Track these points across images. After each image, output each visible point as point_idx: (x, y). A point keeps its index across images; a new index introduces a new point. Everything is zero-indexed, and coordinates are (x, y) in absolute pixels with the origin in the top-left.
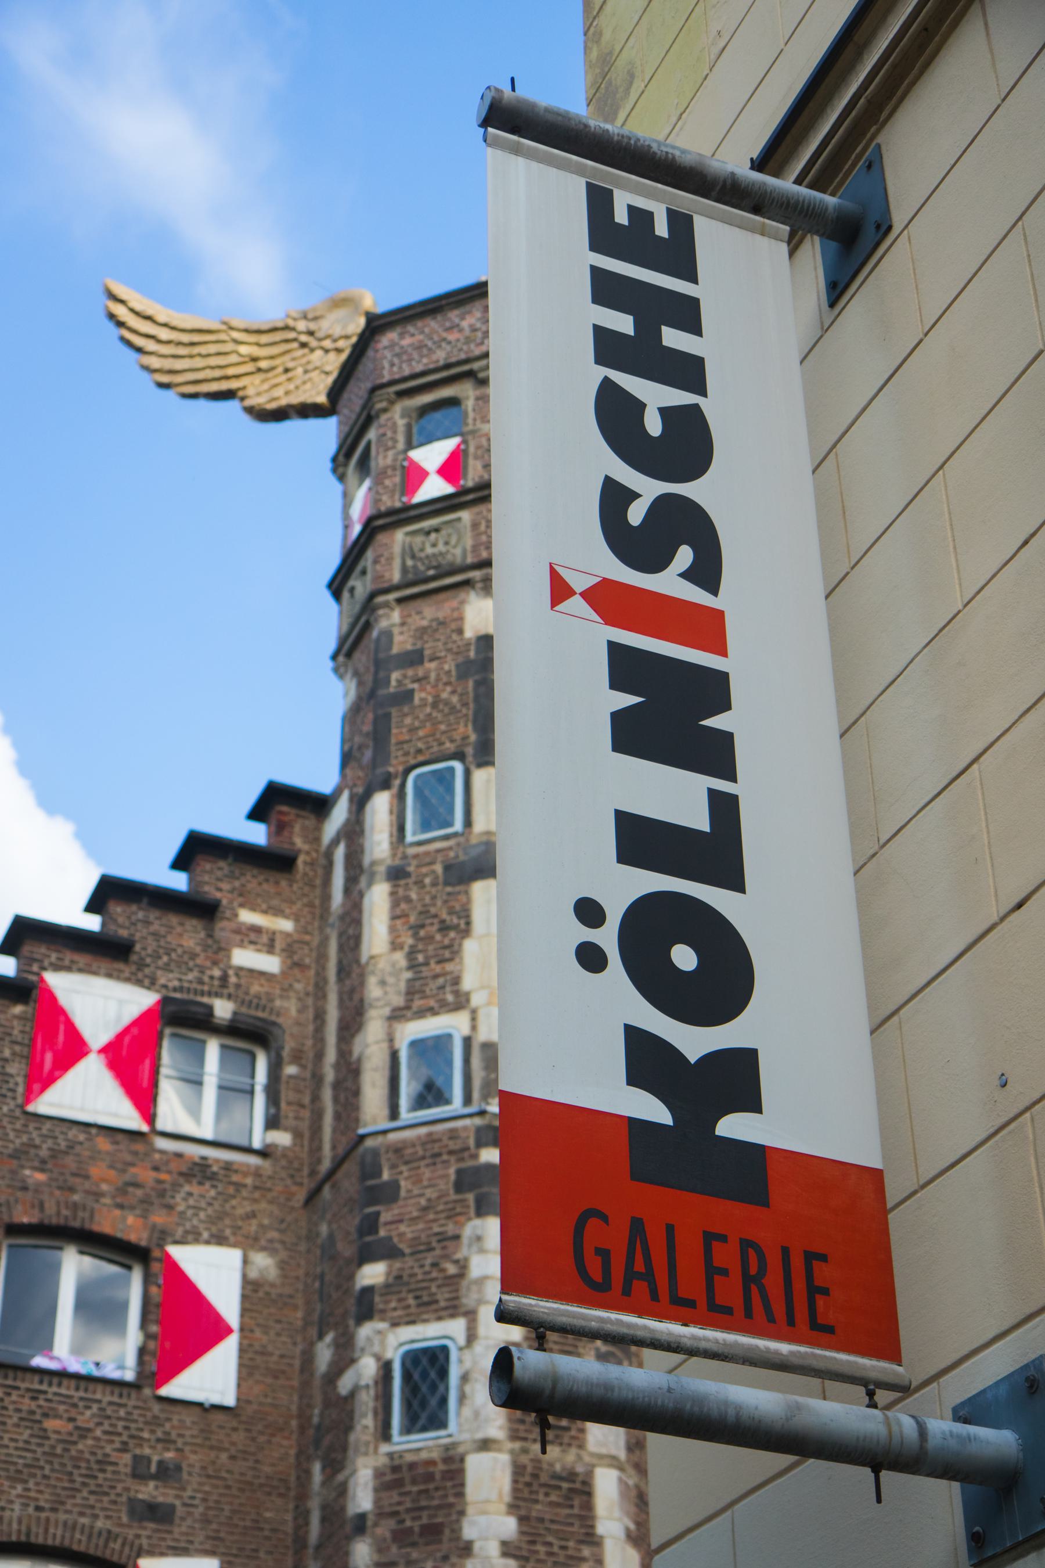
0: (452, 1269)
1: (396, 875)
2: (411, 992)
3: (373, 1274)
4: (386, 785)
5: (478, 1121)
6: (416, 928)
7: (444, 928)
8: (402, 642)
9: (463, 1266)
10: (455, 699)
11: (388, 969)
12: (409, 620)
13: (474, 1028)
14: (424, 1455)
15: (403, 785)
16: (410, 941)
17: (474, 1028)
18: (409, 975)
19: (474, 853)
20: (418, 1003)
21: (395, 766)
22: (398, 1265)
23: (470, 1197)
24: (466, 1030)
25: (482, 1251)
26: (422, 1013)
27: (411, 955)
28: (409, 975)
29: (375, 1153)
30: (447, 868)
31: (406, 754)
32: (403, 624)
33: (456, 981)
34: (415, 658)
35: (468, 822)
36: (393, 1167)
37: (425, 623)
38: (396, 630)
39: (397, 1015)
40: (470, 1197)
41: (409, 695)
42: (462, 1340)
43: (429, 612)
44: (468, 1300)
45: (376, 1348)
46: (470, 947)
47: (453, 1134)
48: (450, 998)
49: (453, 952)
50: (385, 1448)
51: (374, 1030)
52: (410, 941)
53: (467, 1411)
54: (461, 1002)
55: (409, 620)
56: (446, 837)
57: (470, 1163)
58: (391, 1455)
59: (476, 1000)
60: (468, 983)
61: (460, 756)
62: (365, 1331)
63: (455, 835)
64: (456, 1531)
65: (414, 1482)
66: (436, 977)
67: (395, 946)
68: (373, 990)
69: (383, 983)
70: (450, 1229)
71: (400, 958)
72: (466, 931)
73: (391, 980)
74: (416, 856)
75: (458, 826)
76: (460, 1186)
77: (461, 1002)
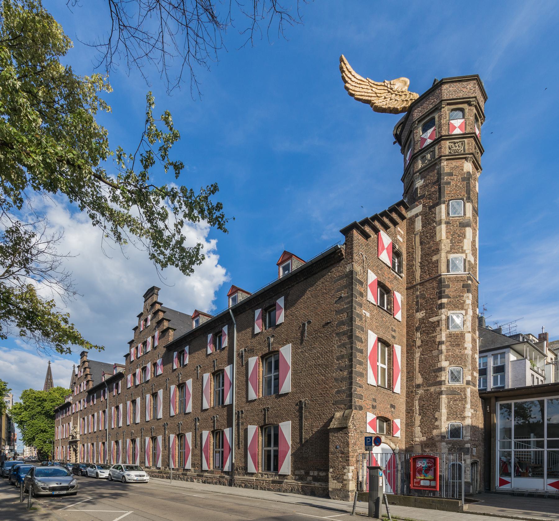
0: (462, 302)
1: (447, 223)
2: (451, 249)
3: (444, 300)
4: (444, 203)
5: (467, 275)
6: (452, 235)
7: (459, 236)
8: (447, 170)
9: (464, 302)
10: (461, 186)
11: (446, 243)
12: (449, 165)
13: (466, 257)
14: (456, 333)
15: (448, 204)
16: (451, 238)
17: (466, 257)
18: (451, 245)
19: (466, 221)
20: (453, 251)
21: (447, 198)
22: (449, 299)
23: (466, 289)
24: (465, 258)
25: (469, 299)
26: (454, 253)
27: (451, 240)
28: (451, 245)
29: (444, 279)
30: (460, 223)
31: (449, 196)
32: (447, 165)
33: (462, 247)
34: (451, 174)
35: (465, 214)
36: (448, 281)
37: (453, 166)
38: (445, 167)
39: (448, 252)
40: (466, 289)
41: (449, 183)
42: (464, 314)
43: (454, 163)
44: (466, 308)
45: (446, 314)
46: (465, 240)
47: (462, 277)
48: (461, 251)
49: (461, 241)
50: (448, 331)
51: (443, 254)
52: (451, 238)
53: (465, 326)
54: (463, 252)
55: (449, 165)
56: (460, 217)
57: (466, 283)
58: (449, 332)
59: (467, 252)
60: (465, 248)
61: (463, 199)
62: (443, 310)
63: (462, 216)
64: (463, 346)
65: (454, 337)
66: (457, 246)
67: (447, 238)
68: (443, 247)
69: (445, 245)
70: (461, 295)
71: (449, 241)
72: (465, 237)
73: (447, 245)
74: (452, 220)
75: (463, 215)
76: (463, 287)
77: (463, 252)
